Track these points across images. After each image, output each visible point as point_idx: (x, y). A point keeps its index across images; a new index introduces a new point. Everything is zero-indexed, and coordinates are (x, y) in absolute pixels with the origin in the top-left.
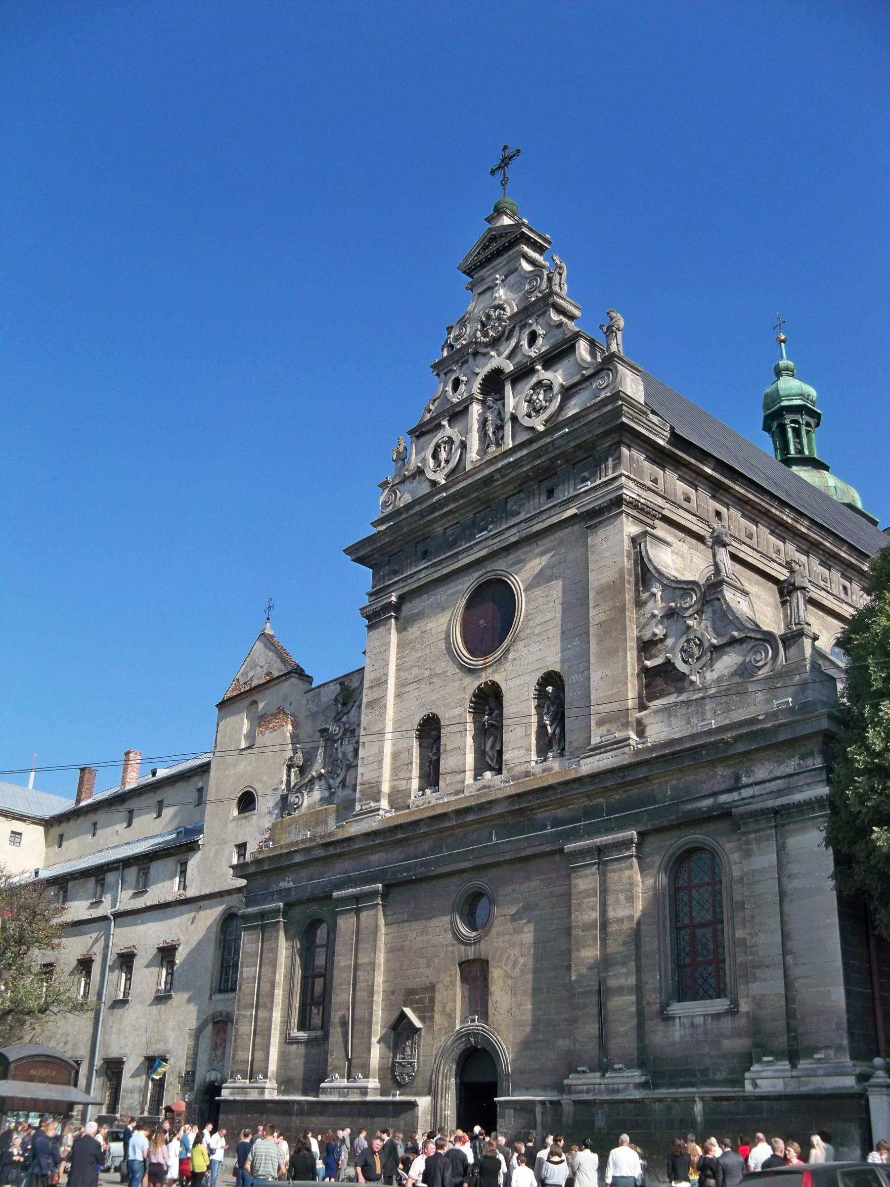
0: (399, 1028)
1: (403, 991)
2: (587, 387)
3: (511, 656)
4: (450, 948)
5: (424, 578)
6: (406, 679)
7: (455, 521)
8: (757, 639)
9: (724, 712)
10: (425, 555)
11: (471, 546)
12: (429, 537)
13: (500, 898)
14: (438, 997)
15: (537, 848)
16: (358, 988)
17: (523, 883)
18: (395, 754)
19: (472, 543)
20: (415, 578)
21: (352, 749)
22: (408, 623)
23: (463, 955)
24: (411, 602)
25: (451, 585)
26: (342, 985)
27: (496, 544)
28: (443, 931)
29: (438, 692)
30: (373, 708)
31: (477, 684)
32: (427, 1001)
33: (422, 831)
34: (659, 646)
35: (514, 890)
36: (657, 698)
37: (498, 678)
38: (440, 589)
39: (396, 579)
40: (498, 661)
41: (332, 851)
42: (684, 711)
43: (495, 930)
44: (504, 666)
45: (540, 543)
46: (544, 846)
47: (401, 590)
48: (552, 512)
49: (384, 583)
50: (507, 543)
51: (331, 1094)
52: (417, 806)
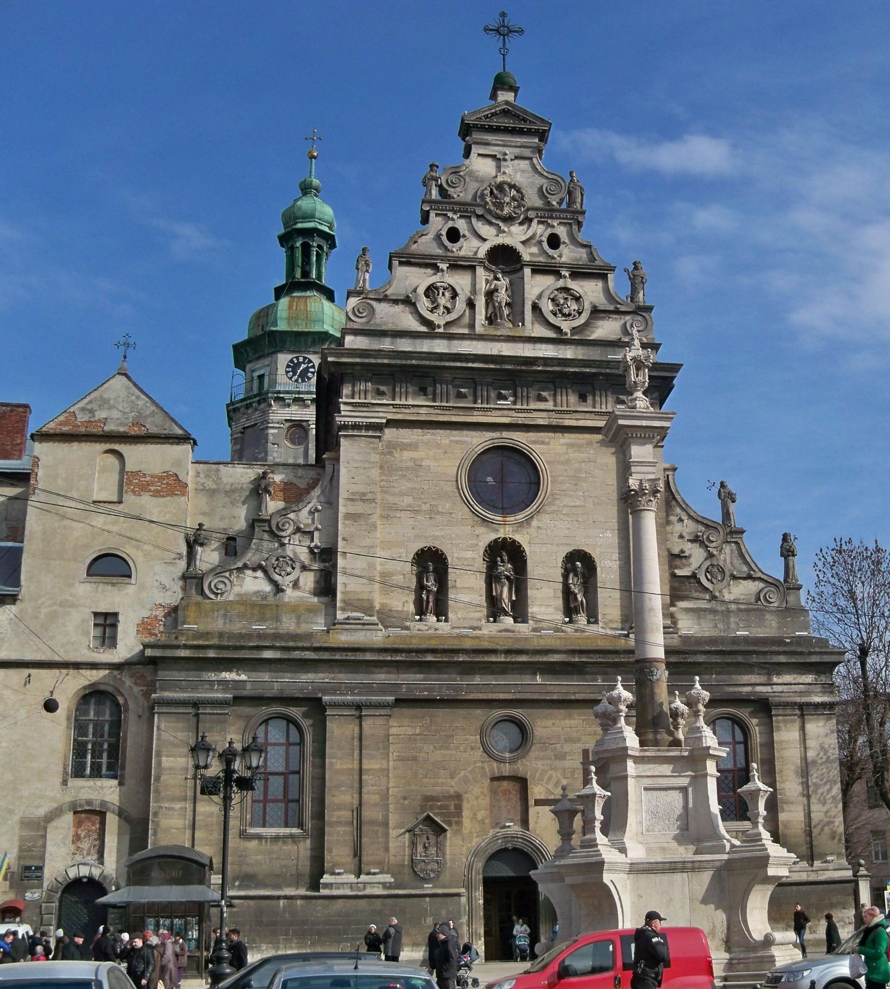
0: (416, 830)
1: (419, 797)
2: (616, 318)
3: (534, 523)
4: (479, 764)
5: (424, 415)
6: (395, 504)
7: (470, 377)
8: (766, 581)
9: (745, 627)
10: (423, 391)
11: (490, 408)
12: (433, 377)
13: (539, 729)
14: (465, 805)
15: (588, 695)
16: (364, 790)
17: (564, 719)
18: (384, 573)
19: (492, 406)
20: (412, 410)
21: (307, 551)
22: (396, 450)
23: (496, 771)
24: (397, 428)
25: (454, 432)
26: (340, 787)
27: (521, 418)
28: (469, 749)
29: (442, 530)
30: (356, 522)
31: (493, 536)
32: (453, 807)
33: (461, 659)
34: (684, 561)
35: (553, 724)
36: (682, 601)
37: (520, 538)
38: (441, 431)
39: (385, 402)
40: (521, 525)
41: (326, 656)
42: (711, 617)
43: (533, 754)
44: (528, 530)
45: (566, 435)
46: (597, 695)
47: (392, 414)
48: (588, 416)
49: (365, 399)
50: (534, 423)
51: (339, 888)
52: (419, 630)
